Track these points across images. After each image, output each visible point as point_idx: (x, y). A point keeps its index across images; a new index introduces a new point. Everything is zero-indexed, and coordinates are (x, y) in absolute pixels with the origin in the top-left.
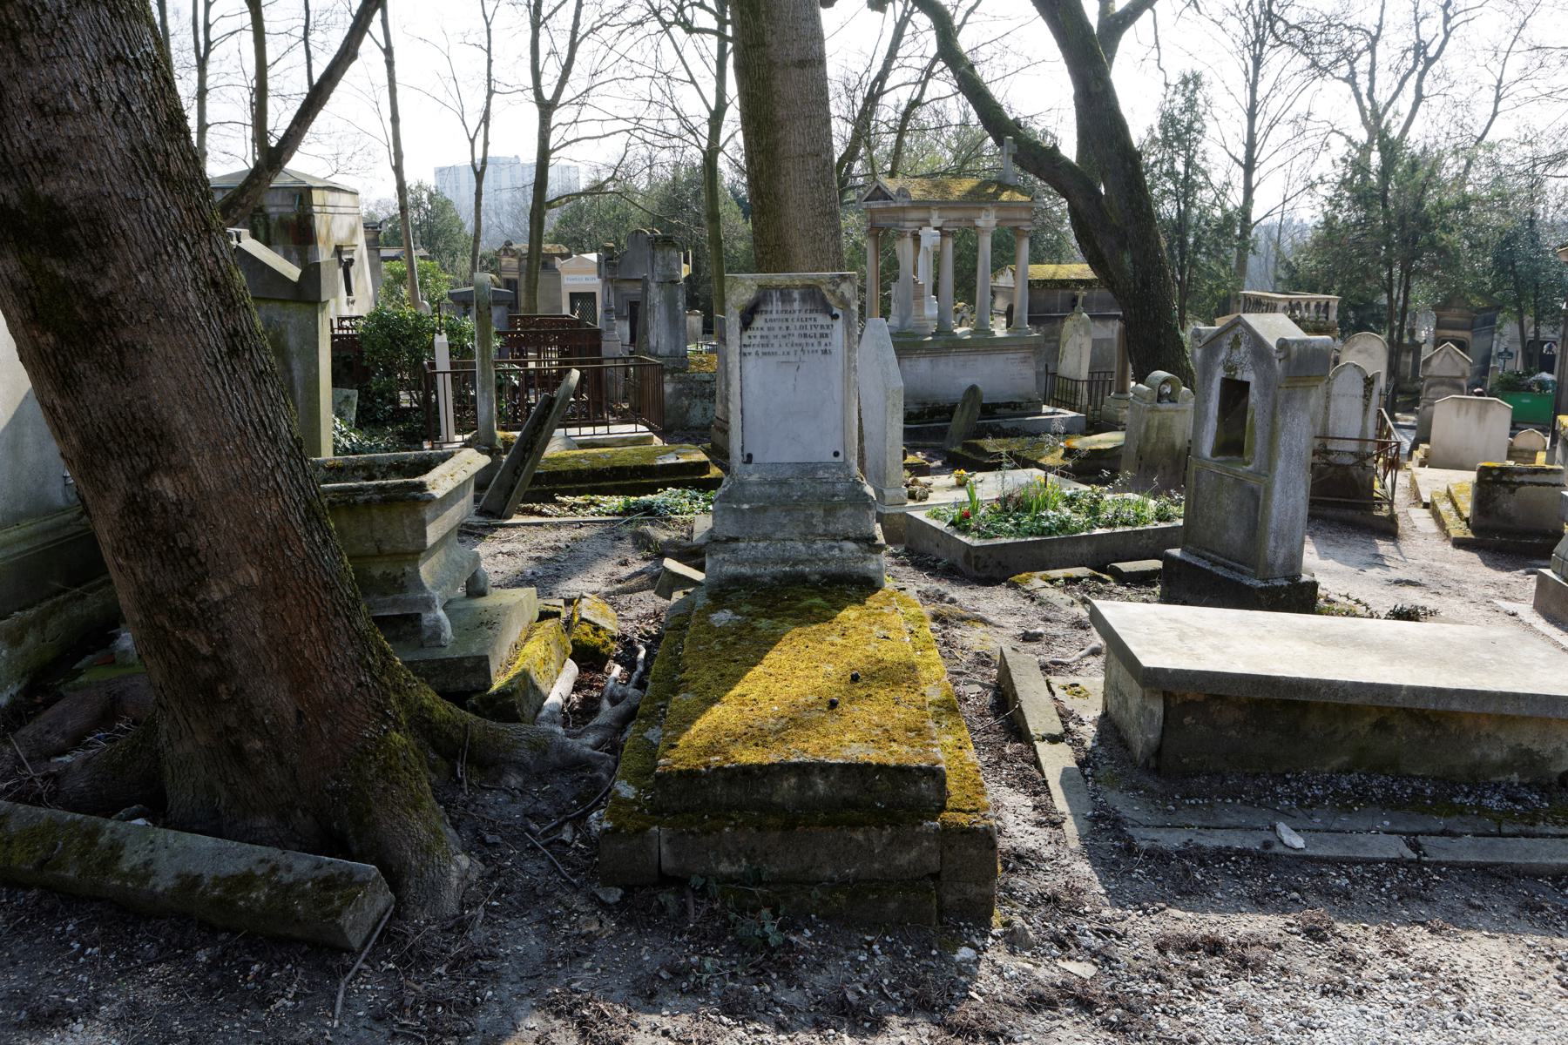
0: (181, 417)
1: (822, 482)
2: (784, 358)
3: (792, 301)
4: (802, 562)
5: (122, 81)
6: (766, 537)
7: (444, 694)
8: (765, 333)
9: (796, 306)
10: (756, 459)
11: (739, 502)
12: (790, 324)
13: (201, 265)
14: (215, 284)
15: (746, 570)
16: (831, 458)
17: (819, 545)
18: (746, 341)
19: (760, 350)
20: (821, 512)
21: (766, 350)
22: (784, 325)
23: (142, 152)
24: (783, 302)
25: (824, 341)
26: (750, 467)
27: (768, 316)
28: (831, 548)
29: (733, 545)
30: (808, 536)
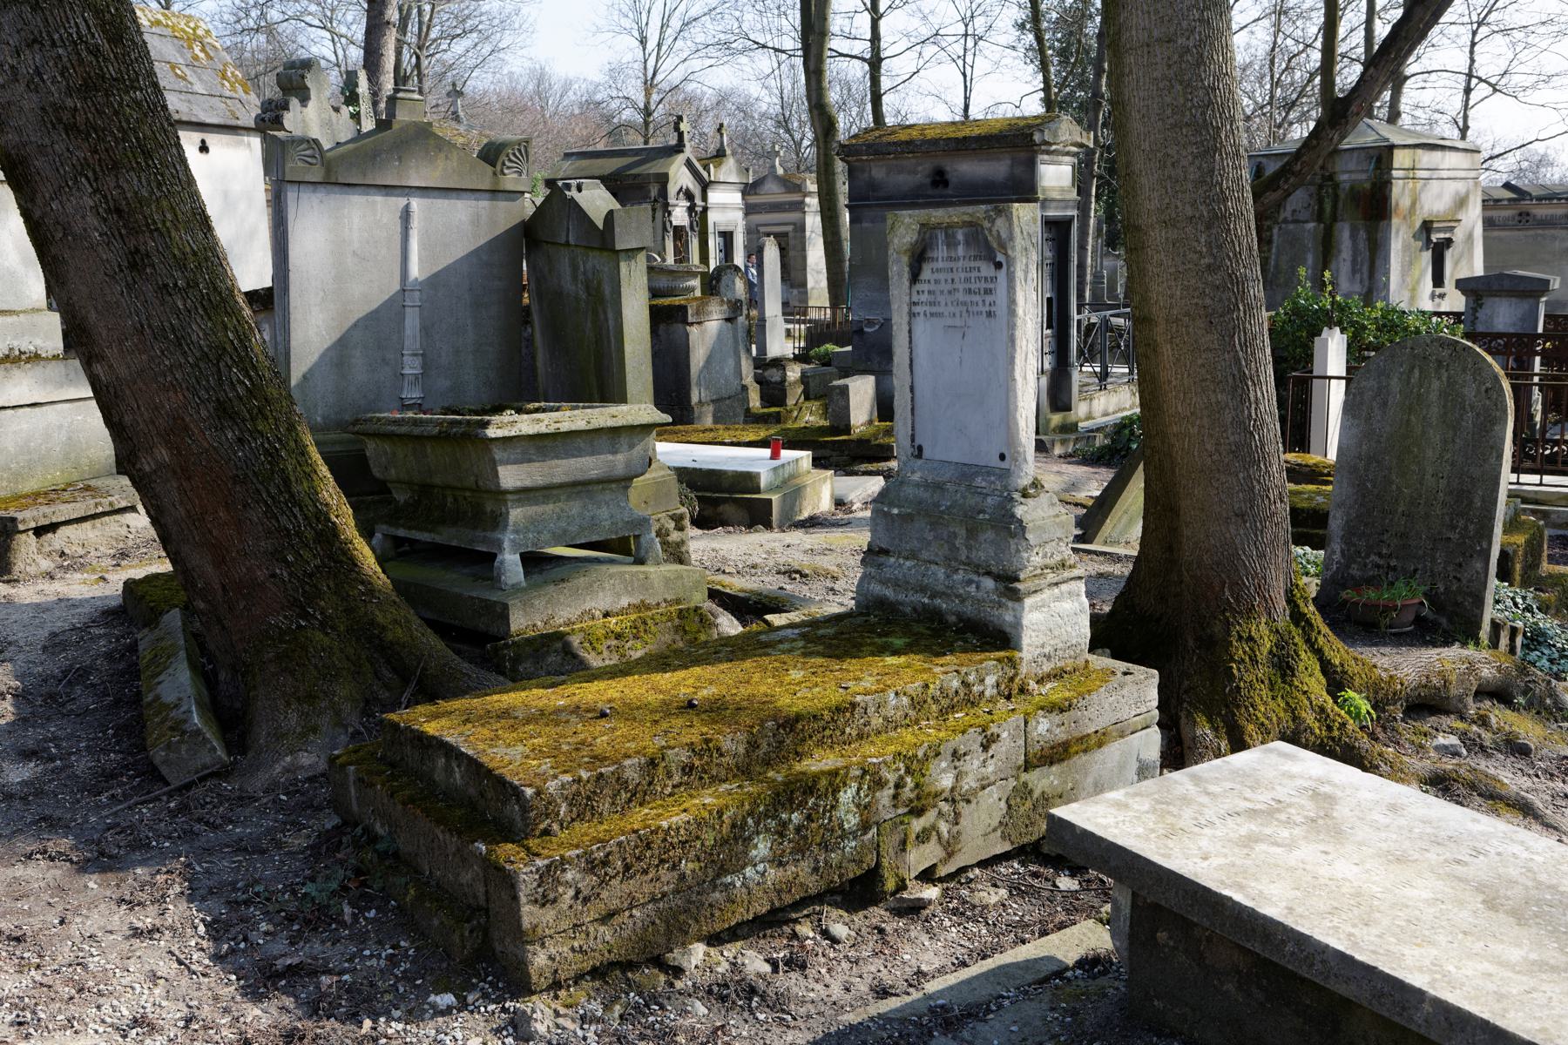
0: (93, 316)
1: (976, 491)
2: (950, 322)
3: (956, 244)
4: (942, 595)
5: (38, 57)
6: (912, 555)
7: (431, 623)
8: (932, 287)
9: (961, 250)
10: (926, 453)
11: (891, 505)
12: (955, 276)
13: (105, 197)
14: (118, 211)
15: (889, 593)
16: (995, 462)
17: (959, 577)
18: (915, 299)
19: (928, 309)
20: (963, 532)
21: (934, 309)
22: (949, 276)
23: (50, 110)
24: (948, 246)
25: (989, 299)
26: (919, 462)
27: (935, 265)
28: (970, 582)
29: (882, 559)
30: (952, 563)
